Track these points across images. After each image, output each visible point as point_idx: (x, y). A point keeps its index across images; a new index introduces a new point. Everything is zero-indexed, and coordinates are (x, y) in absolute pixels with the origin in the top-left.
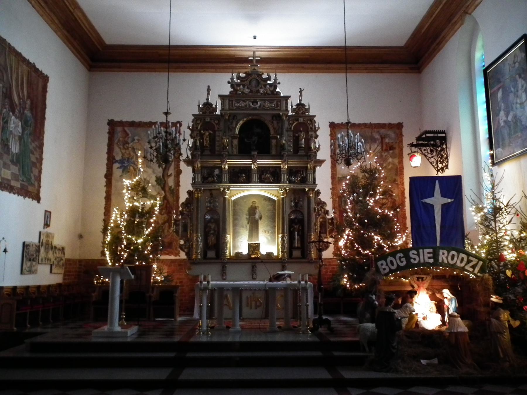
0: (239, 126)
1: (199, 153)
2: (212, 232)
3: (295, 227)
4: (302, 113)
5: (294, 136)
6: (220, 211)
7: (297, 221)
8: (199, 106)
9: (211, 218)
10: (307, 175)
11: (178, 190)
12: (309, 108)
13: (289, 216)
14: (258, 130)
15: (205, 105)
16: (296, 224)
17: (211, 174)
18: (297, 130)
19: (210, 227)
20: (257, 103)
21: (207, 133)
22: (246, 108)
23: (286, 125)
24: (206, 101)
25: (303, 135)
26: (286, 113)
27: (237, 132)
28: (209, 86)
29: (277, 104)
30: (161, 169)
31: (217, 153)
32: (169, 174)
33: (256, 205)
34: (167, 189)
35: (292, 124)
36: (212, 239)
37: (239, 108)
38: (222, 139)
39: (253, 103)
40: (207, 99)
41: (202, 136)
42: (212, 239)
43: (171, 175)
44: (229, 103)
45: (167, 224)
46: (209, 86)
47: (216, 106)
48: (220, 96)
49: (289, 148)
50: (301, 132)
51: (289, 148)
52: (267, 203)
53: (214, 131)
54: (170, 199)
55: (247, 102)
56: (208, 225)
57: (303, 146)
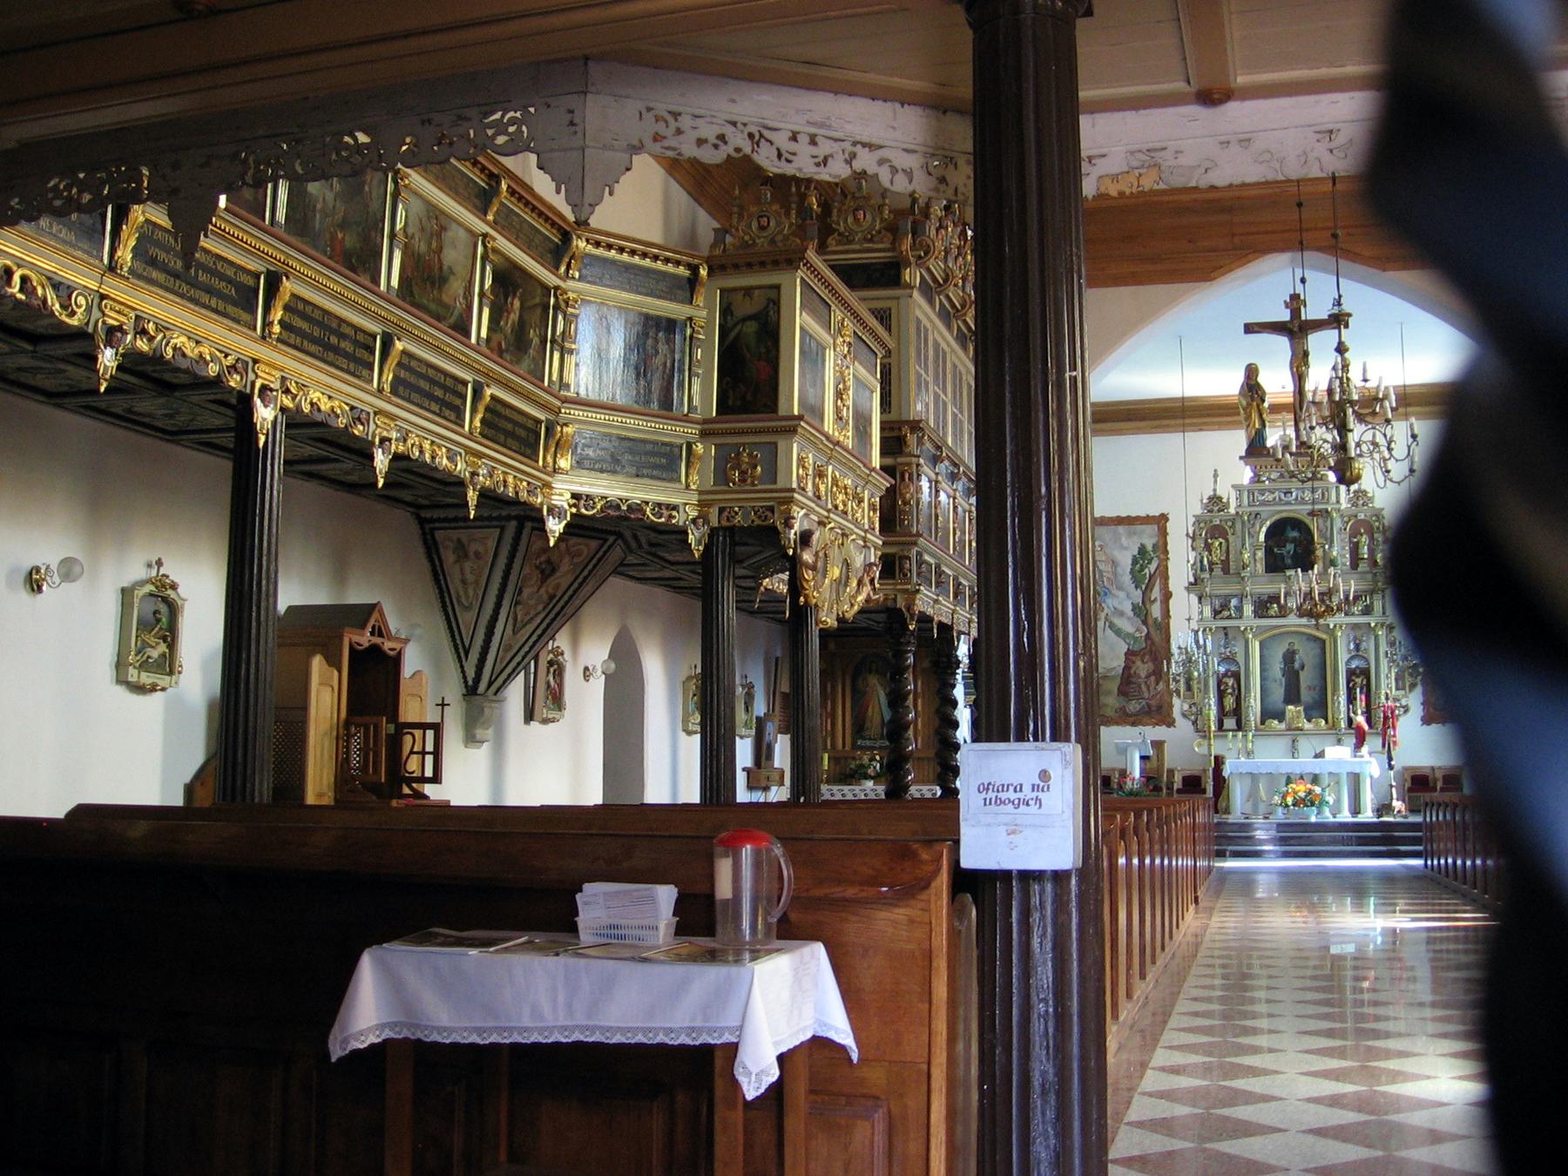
0: (1264, 529)
1: (1208, 576)
2: (1230, 691)
3: (1357, 680)
4: (1363, 505)
5: (1350, 542)
6: (1240, 659)
7: (1358, 671)
8: (1202, 500)
9: (1227, 671)
10: (1372, 603)
11: (1168, 624)
12: (1373, 496)
13: (1348, 662)
14: (1295, 534)
15: (1210, 499)
16: (1358, 677)
17: (1225, 606)
18: (1355, 533)
19: (1227, 684)
20: (1291, 493)
21: (1217, 543)
22: (1274, 502)
23: (1338, 524)
24: (1212, 493)
25: (1364, 539)
26: (1337, 506)
27: (1262, 537)
28: (1215, 471)
29: (1323, 494)
30: (1139, 592)
31: (1231, 572)
32: (1152, 599)
33: (1296, 648)
34: (1150, 622)
35: (1347, 523)
36: (1229, 702)
37: (1264, 503)
38: (1241, 553)
39: (1285, 493)
40: (1215, 490)
41: (1208, 547)
42: (1229, 702)
43: (1155, 600)
44: (1249, 498)
45: (1153, 678)
46: (1215, 471)
47: (1228, 499)
48: (1233, 486)
49: (1344, 560)
50: (1362, 535)
51: (1344, 560)
52: (1312, 644)
53: (1227, 540)
54: (1157, 637)
55: (1277, 494)
56: (1224, 680)
57: (1366, 556)
